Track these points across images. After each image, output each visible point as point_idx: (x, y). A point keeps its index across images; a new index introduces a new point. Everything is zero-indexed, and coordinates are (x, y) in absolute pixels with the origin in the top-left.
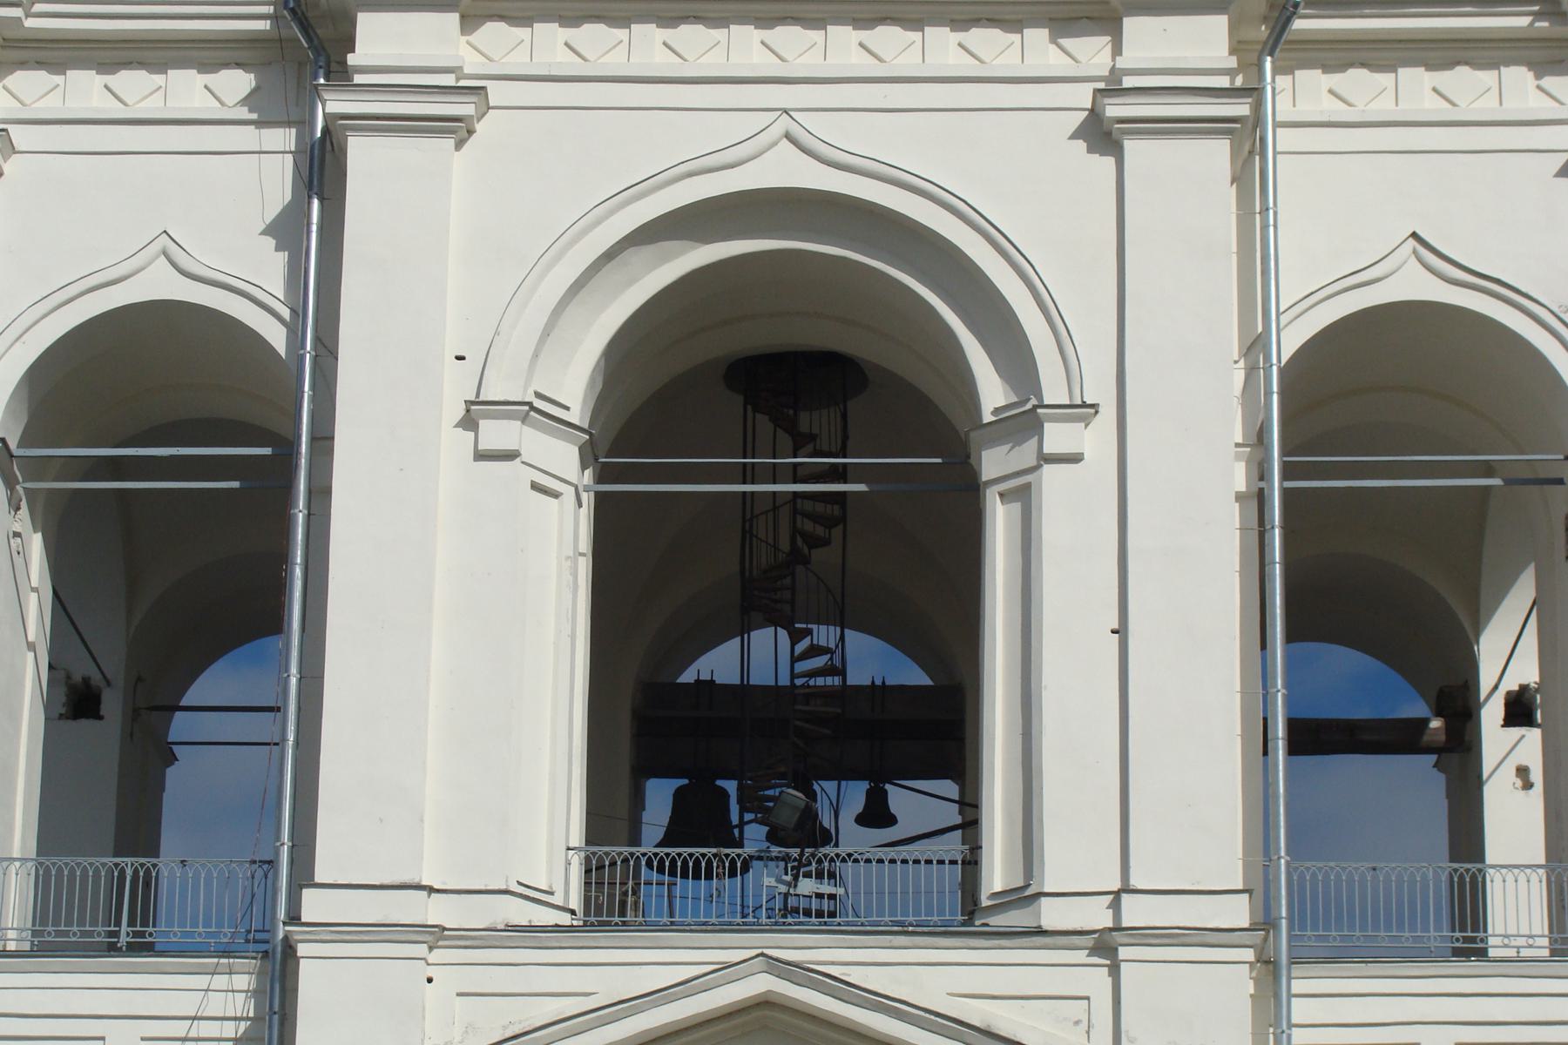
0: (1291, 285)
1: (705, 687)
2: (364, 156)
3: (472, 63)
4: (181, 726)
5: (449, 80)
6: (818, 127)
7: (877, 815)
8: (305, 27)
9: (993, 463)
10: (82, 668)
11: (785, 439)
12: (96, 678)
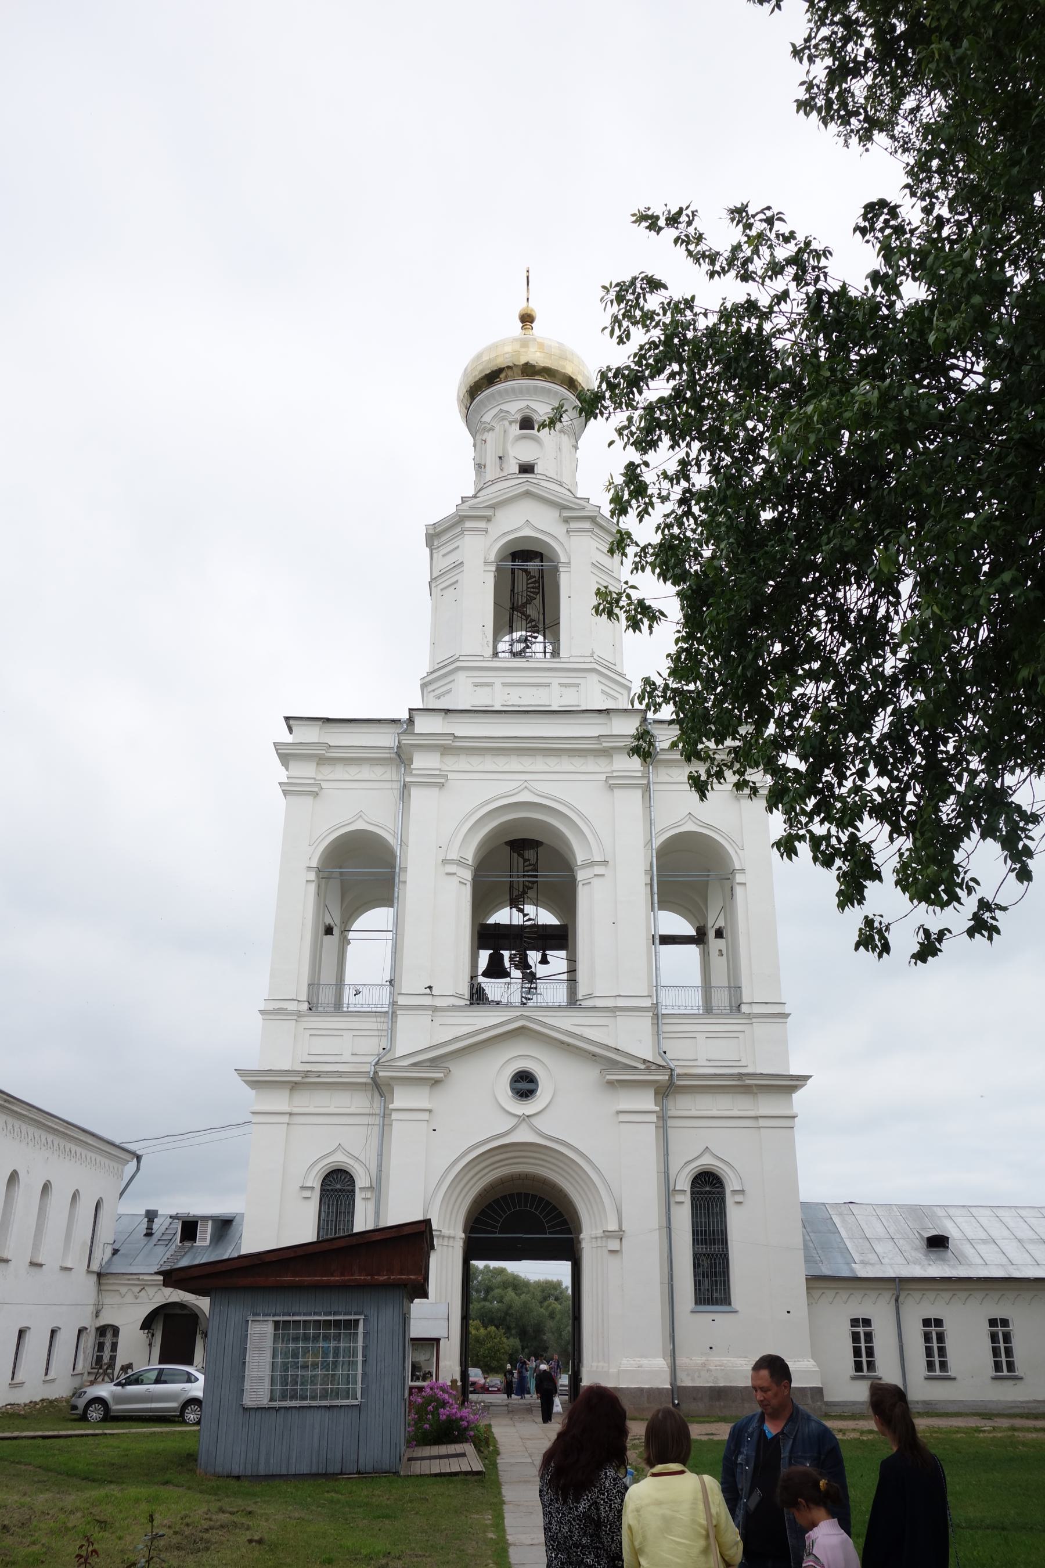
0: (657, 827)
1: (497, 925)
2: (415, 792)
3: (445, 768)
4: (351, 935)
5: (437, 773)
6: (534, 784)
7: (544, 961)
8: (399, 756)
9: (581, 875)
10: (328, 921)
11: (521, 860)
12: (332, 924)
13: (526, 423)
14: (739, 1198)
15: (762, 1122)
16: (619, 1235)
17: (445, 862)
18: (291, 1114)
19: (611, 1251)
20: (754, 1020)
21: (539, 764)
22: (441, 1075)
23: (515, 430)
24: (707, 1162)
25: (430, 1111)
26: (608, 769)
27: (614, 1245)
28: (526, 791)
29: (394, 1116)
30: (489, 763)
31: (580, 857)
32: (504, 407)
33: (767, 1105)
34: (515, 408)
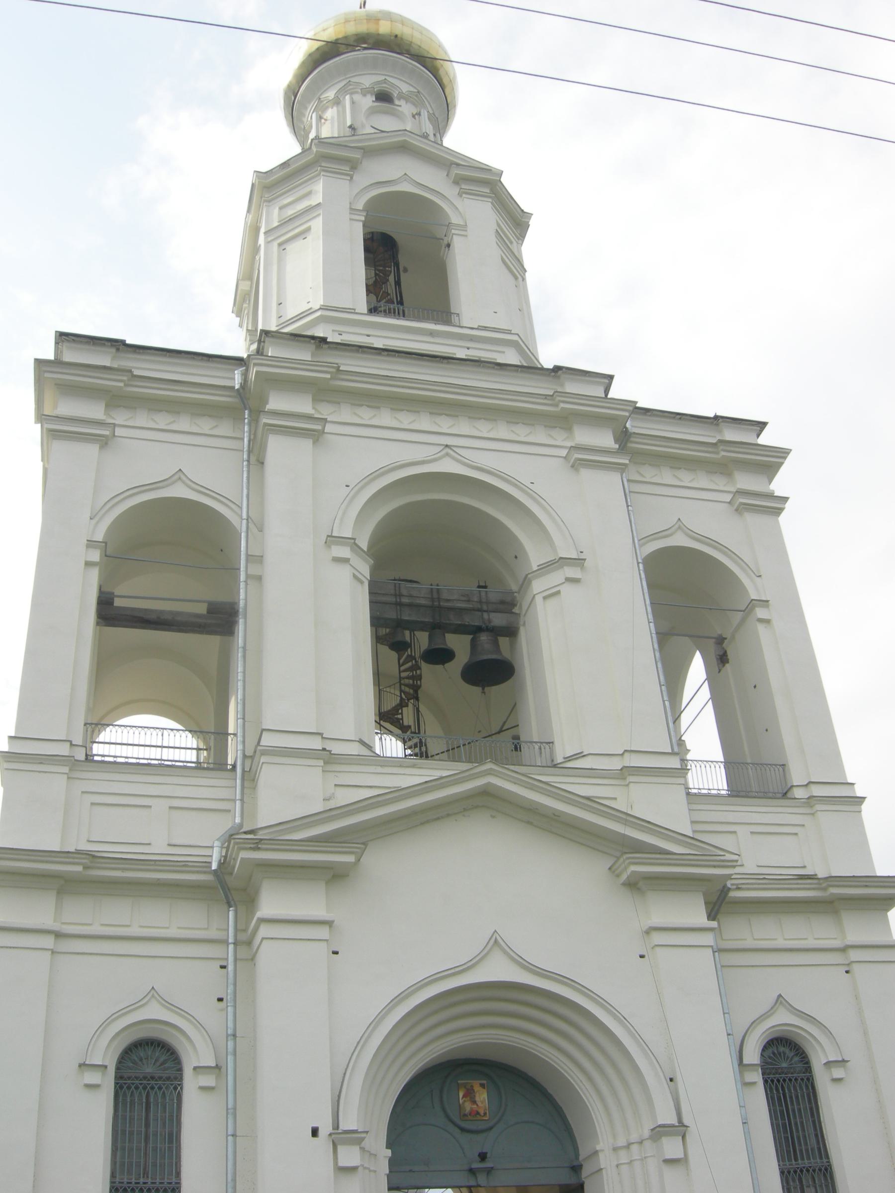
13: (384, 97)
14: (838, 1073)
15: (854, 955)
16: (680, 1129)
17: (332, 540)
18: (58, 935)
19: (668, 1162)
20: (818, 807)
21: (464, 426)
22: (351, 859)
23: (368, 101)
24: (782, 1019)
25: (329, 923)
26: (569, 444)
27: (672, 1147)
28: (447, 460)
29: (264, 931)
30: (386, 417)
31: (535, 556)
32: (353, 80)
33: (856, 929)
34: (368, 80)
